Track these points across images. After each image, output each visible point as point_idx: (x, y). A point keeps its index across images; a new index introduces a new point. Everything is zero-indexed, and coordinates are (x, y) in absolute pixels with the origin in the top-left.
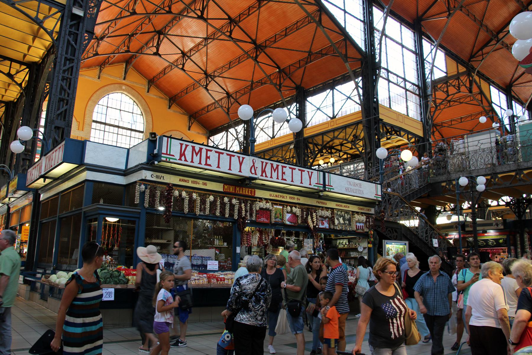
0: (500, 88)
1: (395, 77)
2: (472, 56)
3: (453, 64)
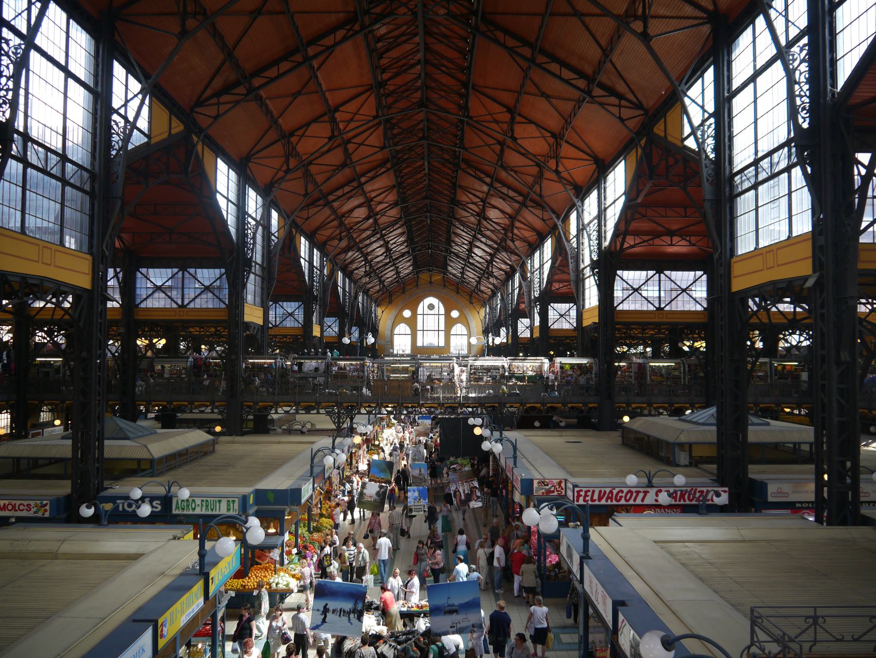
0: (231, 163)
3: (163, 114)
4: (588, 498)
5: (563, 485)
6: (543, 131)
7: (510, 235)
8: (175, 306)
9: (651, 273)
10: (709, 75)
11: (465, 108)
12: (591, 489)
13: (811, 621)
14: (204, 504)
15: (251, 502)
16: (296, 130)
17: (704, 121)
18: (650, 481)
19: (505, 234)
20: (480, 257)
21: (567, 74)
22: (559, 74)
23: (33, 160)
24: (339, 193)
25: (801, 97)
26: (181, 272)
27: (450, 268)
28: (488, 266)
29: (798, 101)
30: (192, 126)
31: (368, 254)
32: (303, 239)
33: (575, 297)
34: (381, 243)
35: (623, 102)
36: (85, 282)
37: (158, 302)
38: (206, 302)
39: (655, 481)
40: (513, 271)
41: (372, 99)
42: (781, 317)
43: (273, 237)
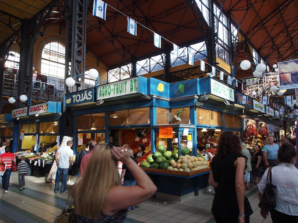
2: (248, 32)
30: (247, 39)
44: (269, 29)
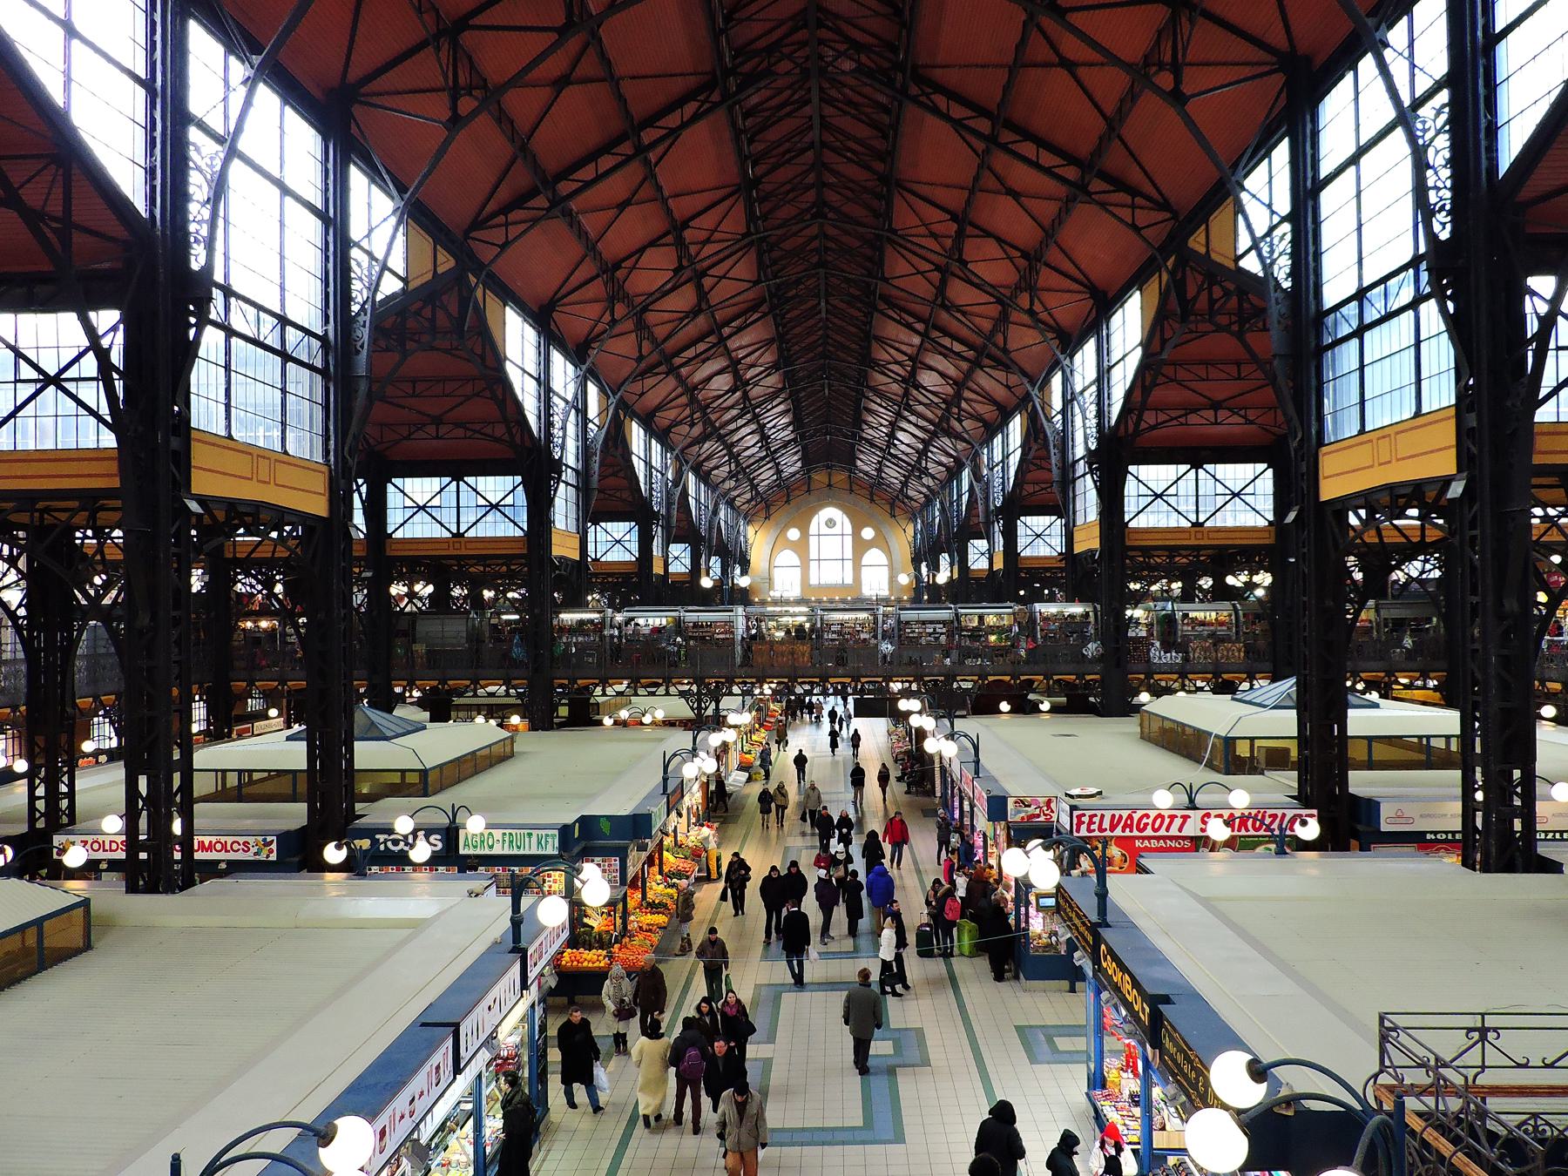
1: (251, 311)
2: (478, 223)
3: (426, 243)
4: (1092, 827)
5: (1053, 805)
6: (1009, 249)
7: (955, 410)
8: (447, 535)
9: (1183, 468)
10: (1282, 152)
11: (888, 215)
12: (1099, 813)
13: (1476, 1035)
14: (507, 839)
15: (576, 835)
16: (624, 260)
17: (1272, 229)
18: (1191, 800)
19: (947, 410)
20: (908, 445)
21: (1047, 159)
22: (1034, 159)
23: (237, 323)
24: (690, 353)
25: (1438, 189)
26: (454, 483)
27: (859, 463)
28: (919, 459)
29: (1433, 197)
30: (467, 261)
31: (733, 445)
32: (635, 426)
33: (1061, 507)
34: (754, 427)
35: (1138, 200)
36: (318, 506)
37: (422, 528)
38: (497, 528)
39: (1200, 799)
40: (960, 466)
41: (740, 205)
42: (1397, 533)
43: (591, 425)
44: (590, 223)
